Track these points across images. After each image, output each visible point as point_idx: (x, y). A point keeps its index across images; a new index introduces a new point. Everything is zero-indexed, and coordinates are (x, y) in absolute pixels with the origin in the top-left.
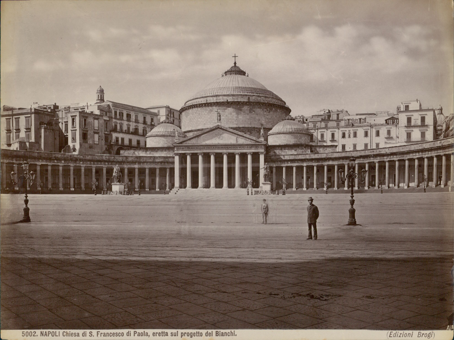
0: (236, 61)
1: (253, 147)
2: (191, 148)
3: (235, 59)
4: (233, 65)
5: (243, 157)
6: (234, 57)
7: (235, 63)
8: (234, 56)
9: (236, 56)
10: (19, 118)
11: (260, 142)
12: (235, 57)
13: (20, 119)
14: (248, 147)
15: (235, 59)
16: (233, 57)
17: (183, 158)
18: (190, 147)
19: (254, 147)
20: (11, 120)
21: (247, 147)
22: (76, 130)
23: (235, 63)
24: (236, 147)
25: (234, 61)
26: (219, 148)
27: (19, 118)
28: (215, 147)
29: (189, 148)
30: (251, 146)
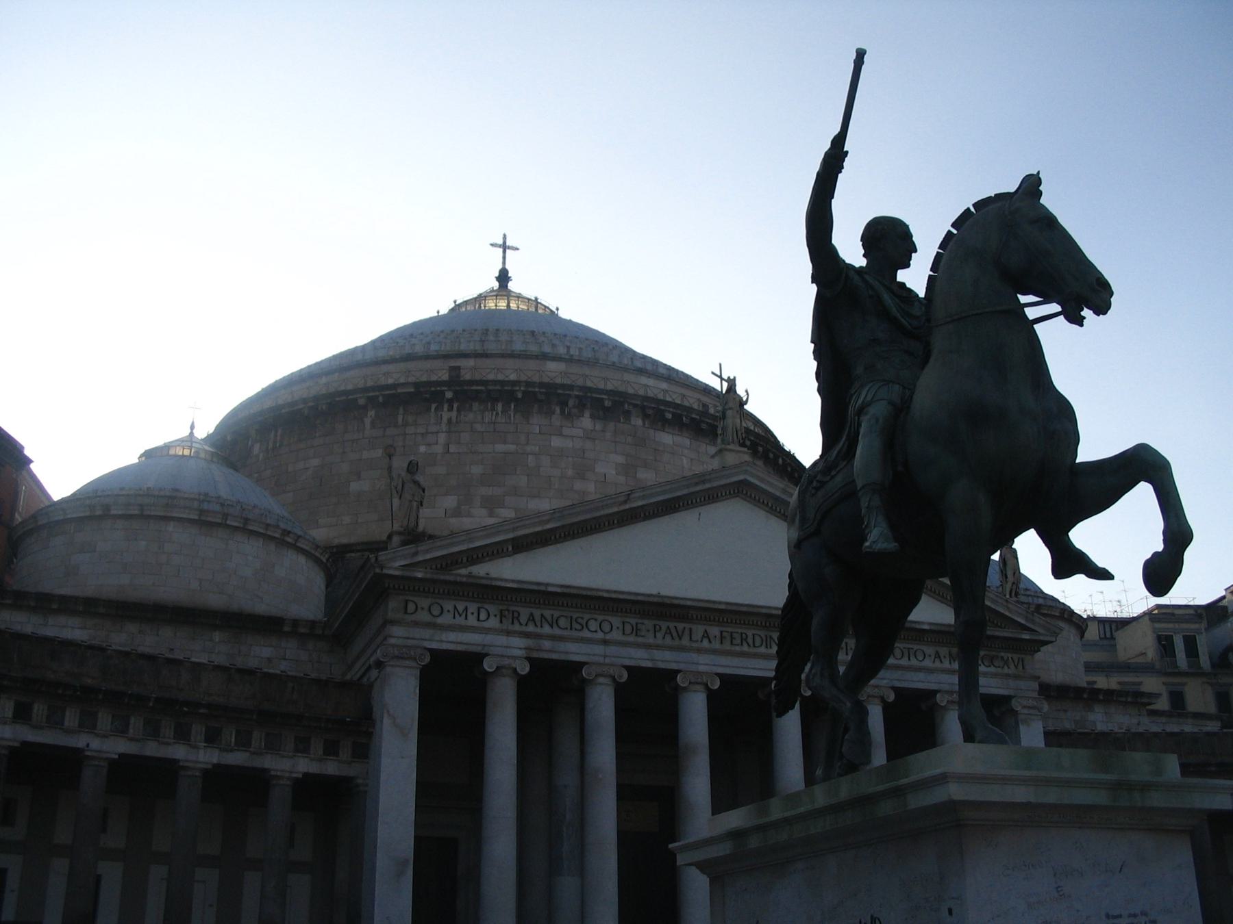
0: (507, 267)
2: (532, 618)
3: (504, 258)
4: (496, 285)
6: (501, 250)
7: (503, 277)
9: (501, 242)
12: (505, 247)
14: (937, 655)
15: (504, 258)
16: (505, 237)
18: (524, 613)
21: (930, 650)
23: (503, 277)
25: (500, 267)
26: (744, 639)
28: (714, 631)
29: (515, 617)
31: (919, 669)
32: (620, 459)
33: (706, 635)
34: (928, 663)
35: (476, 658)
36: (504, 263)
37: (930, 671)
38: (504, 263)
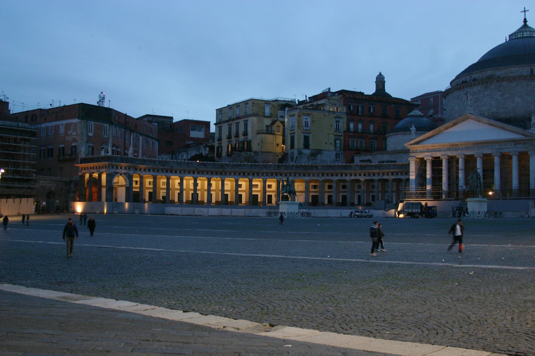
0: (526, 18)
1: (519, 144)
4: (523, 23)
5: (505, 158)
6: (524, 13)
7: (525, 21)
8: (526, 10)
10: (239, 122)
11: (529, 136)
12: (525, 11)
13: (240, 124)
16: (522, 12)
17: (422, 163)
19: (521, 144)
20: (233, 125)
22: (295, 133)
23: (525, 21)
24: (494, 146)
25: (524, 18)
27: (239, 122)
30: (515, 142)
31: (507, 148)
32: (501, 93)
33: (462, 148)
34: (509, 147)
35: (423, 158)
36: (525, 16)
37: (509, 148)
38: (525, 16)
